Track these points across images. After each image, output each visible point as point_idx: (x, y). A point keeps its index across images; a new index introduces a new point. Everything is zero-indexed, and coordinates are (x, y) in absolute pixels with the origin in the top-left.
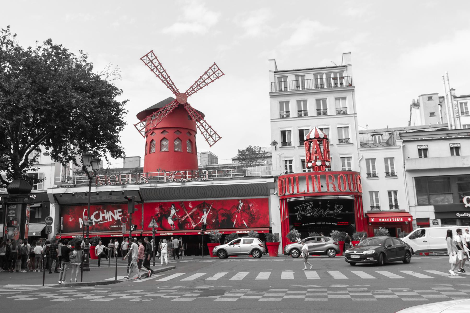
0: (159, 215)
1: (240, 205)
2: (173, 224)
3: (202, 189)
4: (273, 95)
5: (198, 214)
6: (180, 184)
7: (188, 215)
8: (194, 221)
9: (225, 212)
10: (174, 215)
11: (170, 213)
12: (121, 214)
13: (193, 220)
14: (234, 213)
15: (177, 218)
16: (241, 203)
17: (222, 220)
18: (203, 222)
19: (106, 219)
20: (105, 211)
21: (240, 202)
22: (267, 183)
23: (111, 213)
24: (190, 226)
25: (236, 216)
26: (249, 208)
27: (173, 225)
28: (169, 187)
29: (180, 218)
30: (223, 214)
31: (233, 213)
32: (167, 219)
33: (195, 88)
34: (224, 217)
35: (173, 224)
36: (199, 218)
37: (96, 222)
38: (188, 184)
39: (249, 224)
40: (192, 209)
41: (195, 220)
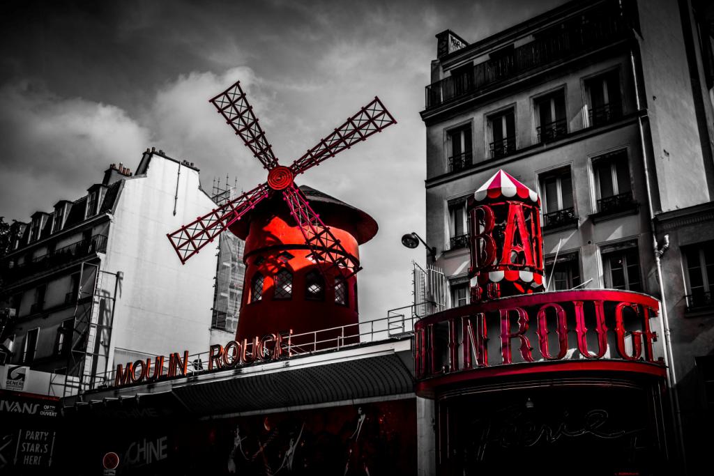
1: (360, 420)
2: (234, 472)
3: (275, 382)
4: (431, 117)
6: (231, 372)
7: (261, 449)
12: (165, 447)
19: (145, 458)
20: (145, 440)
21: (360, 412)
22: (396, 353)
23: (151, 443)
33: (261, 148)
36: (280, 456)
38: (249, 372)
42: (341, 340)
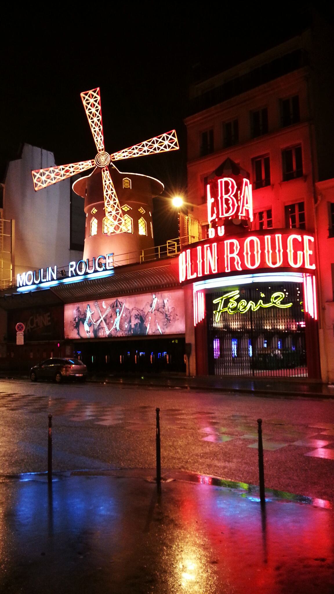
0: (77, 319)
1: (154, 301)
2: (88, 331)
5: (111, 317)
7: (102, 319)
8: (107, 327)
9: (138, 313)
10: (89, 319)
11: (85, 317)
12: (49, 318)
13: (107, 324)
14: (147, 314)
15: (92, 323)
16: (155, 299)
17: (135, 324)
18: (116, 327)
19: (38, 325)
24: (104, 333)
25: (150, 318)
26: (164, 306)
27: (89, 332)
28: (74, 282)
29: (95, 322)
30: (135, 315)
31: (146, 314)
32: (83, 324)
34: (137, 319)
35: (88, 331)
36: (112, 322)
37: (31, 329)
39: (164, 329)
40: (106, 309)
41: (108, 324)
42: (142, 258)
